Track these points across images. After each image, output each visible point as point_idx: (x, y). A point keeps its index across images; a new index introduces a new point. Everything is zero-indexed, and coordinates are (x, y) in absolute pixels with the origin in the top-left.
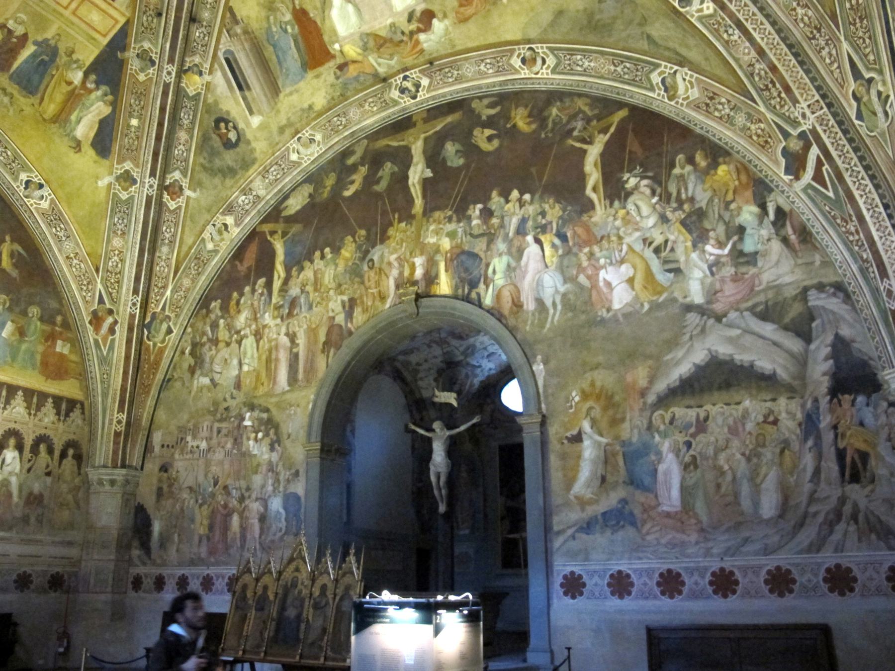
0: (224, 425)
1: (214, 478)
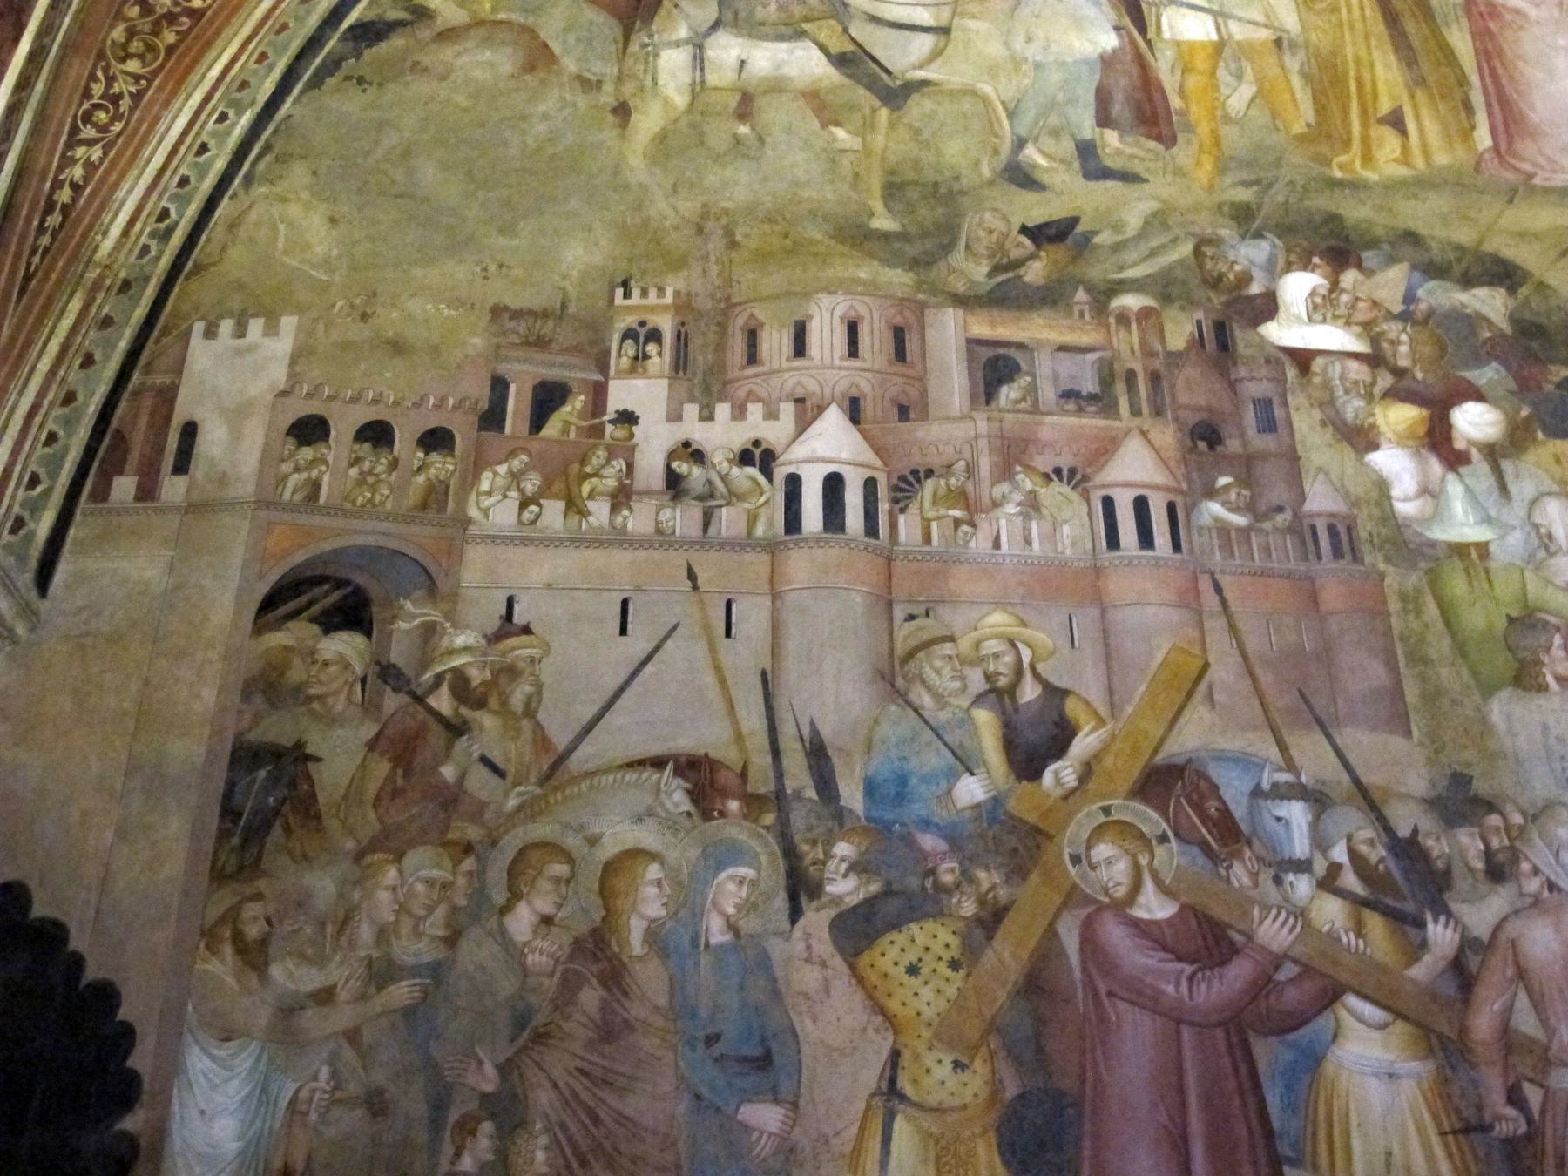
0: (1036, 329)
1: (999, 695)
